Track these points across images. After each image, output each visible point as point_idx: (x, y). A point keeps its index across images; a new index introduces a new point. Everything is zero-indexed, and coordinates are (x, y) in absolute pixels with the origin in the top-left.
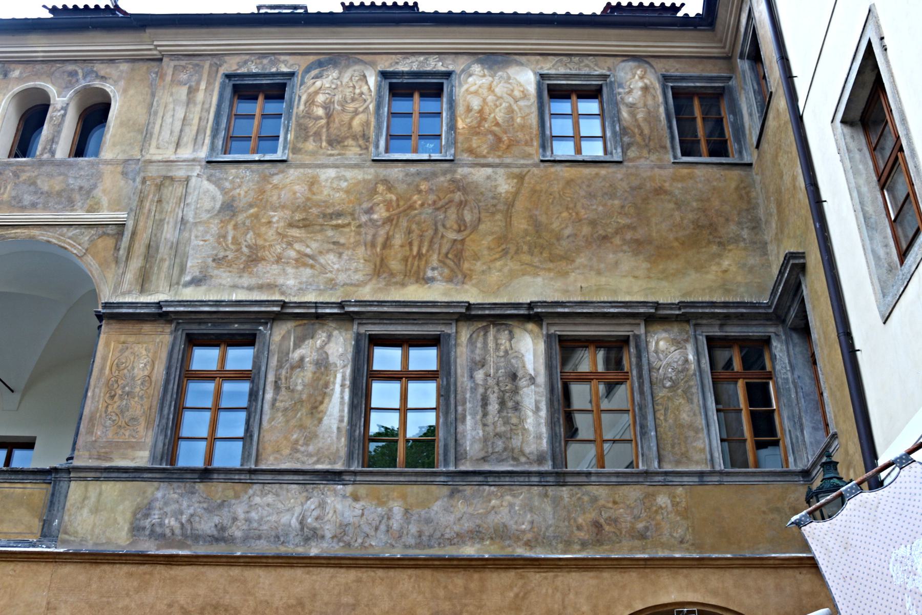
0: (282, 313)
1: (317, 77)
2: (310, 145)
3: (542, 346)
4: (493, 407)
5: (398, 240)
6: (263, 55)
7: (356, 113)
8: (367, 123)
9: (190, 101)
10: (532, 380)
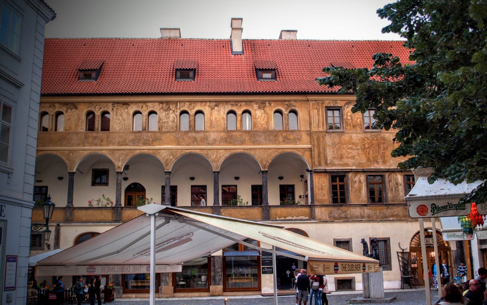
0: (351, 171)
1: (347, 107)
2: (349, 127)
3: (402, 177)
4: (394, 190)
5: (371, 153)
6: (334, 101)
7: (358, 118)
8: (361, 121)
10: (401, 185)
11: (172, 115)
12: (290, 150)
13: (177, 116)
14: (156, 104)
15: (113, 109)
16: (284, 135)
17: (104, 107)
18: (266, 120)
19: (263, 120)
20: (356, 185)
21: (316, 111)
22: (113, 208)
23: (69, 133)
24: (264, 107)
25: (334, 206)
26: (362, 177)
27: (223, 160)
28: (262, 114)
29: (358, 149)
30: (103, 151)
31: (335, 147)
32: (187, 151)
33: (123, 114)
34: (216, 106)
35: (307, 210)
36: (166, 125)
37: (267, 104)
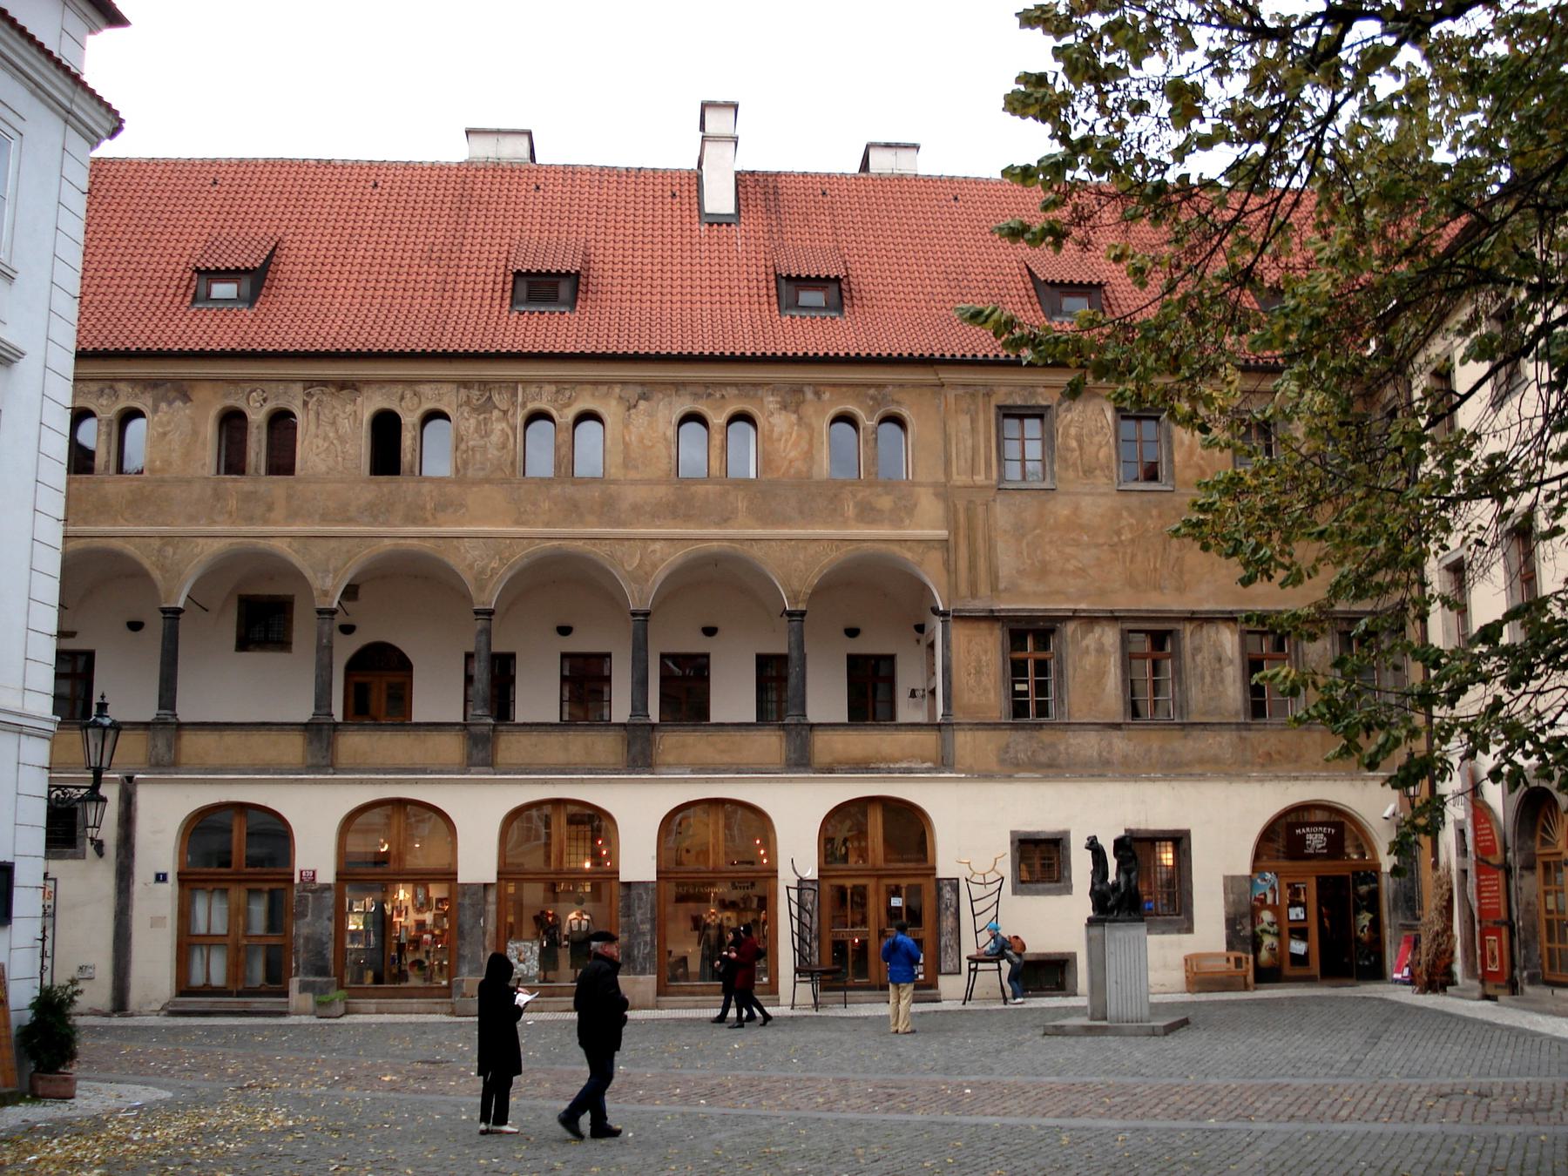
0: (1075, 616)
1: (1068, 410)
2: (1071, 474)
3: (1236, 638)
6: (1024, 387)
7: (1101, 447)
9: (974, 430)
10: (1231, 662)
11: (499, 427)
12: (883, 546)
13: (514, 429)
14: (446, 388)
15: (305, 404)
16: (860, 496)
17: (277, 397)
18: (804, 445)
19: (796, 444)
20: (1089, 661)
21: (965, 421)
22: (305, 727)
23: (163, 481)
24: (798, 405)
25: (1015, 727)
26: (1109, 636)
27: (662, 577)
28: (791, 426)
29: (1097, 546)
30: (273, 542)
31: (1023, 536)
32: (549, 544)
33: (339, 420)
34: (644, 397)
35: (929, 739)
36: (478, 456)
37: (809, 395)
